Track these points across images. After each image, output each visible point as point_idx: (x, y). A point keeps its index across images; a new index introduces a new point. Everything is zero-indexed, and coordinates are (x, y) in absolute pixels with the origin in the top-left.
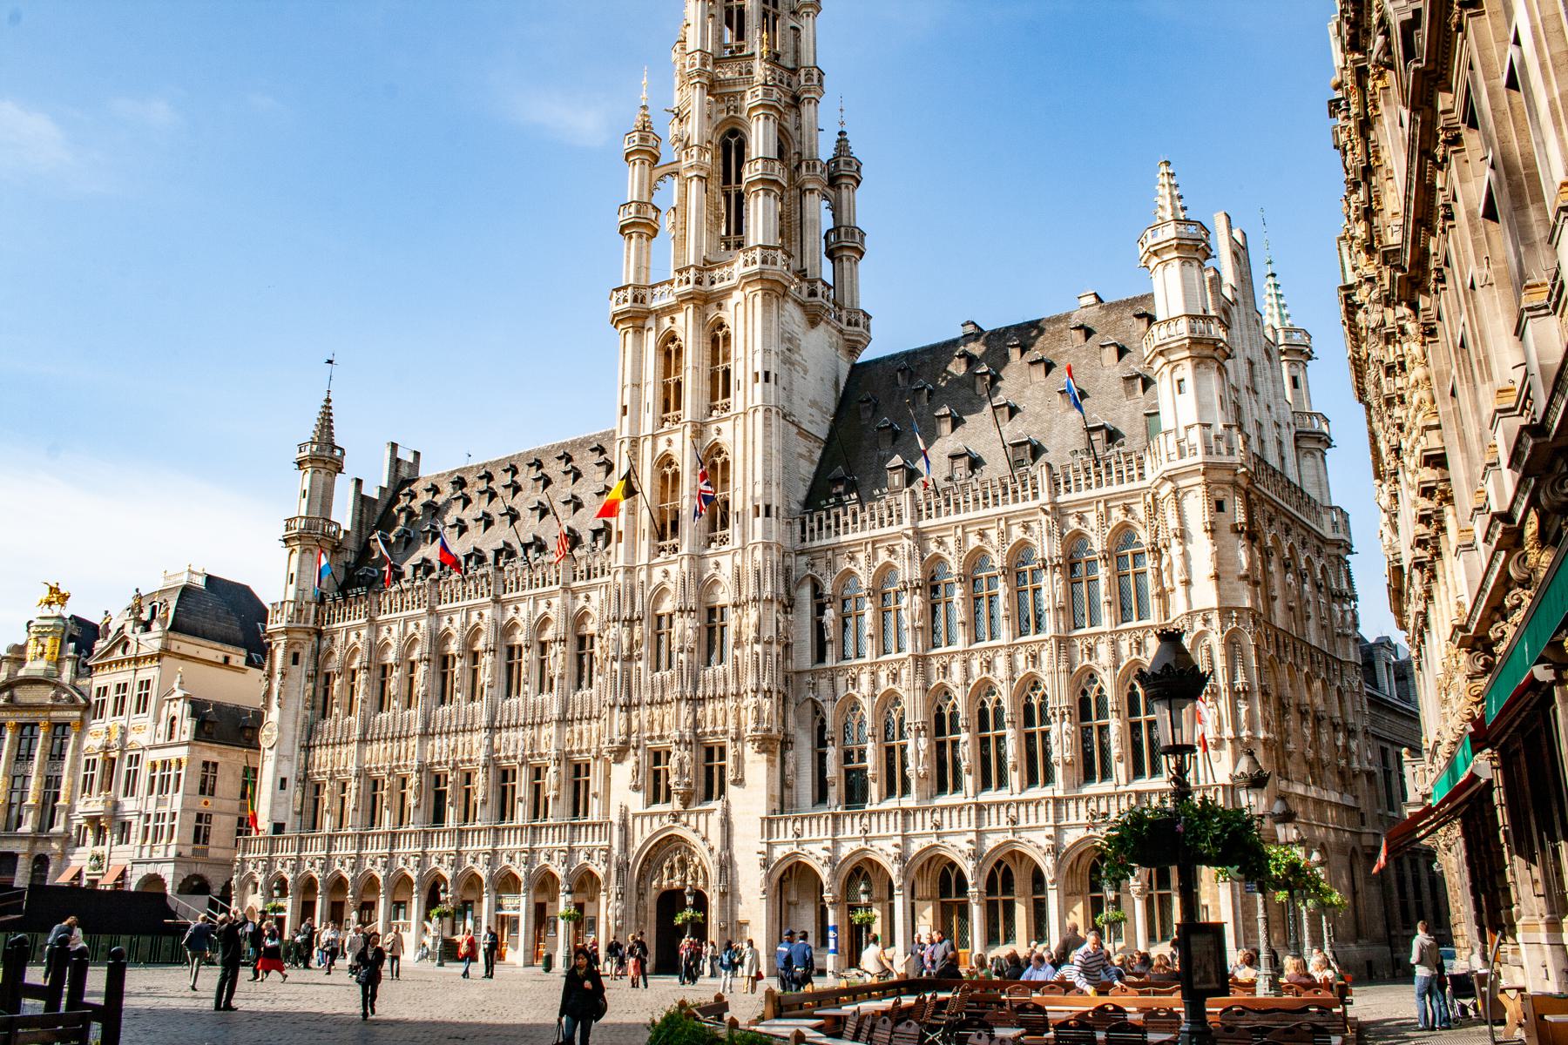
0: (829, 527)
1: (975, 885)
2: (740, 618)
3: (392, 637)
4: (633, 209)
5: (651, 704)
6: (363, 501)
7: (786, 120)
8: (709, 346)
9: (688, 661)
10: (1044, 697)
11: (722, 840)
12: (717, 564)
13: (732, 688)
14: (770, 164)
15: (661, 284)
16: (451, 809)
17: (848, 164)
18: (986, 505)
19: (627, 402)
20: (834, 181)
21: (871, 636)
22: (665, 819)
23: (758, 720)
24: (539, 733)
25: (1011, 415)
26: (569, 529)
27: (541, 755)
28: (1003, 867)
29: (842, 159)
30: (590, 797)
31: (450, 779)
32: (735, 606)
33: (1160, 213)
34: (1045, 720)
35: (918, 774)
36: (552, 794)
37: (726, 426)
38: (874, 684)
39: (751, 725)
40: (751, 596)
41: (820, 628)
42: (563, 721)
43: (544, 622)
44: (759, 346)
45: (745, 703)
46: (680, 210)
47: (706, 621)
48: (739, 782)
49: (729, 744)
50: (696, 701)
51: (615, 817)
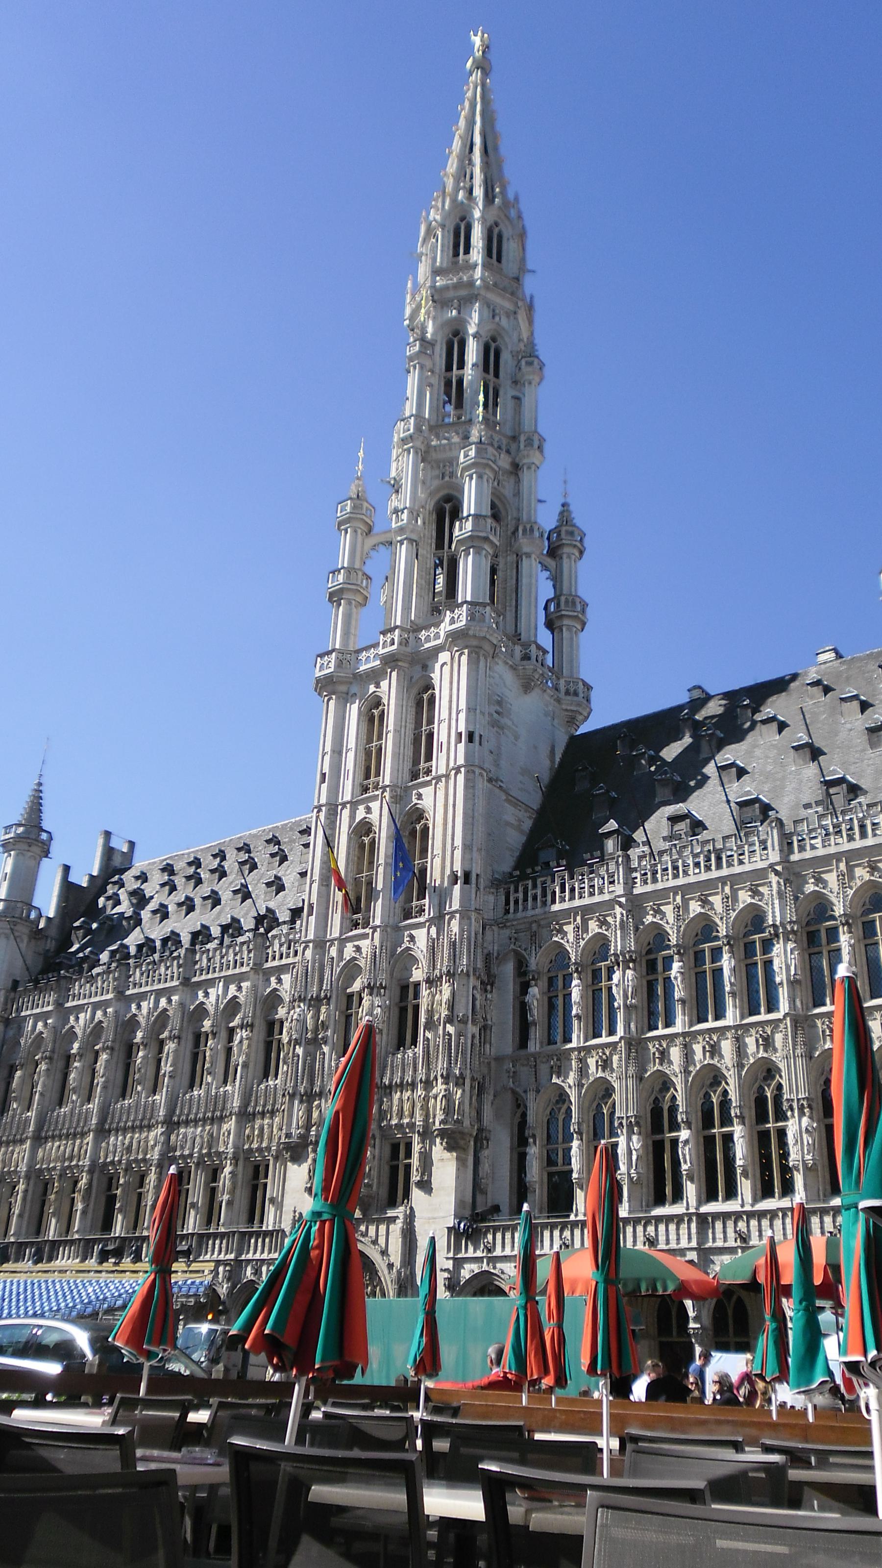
0: (535, 898)
1: (696, 1319)
2: (434, 996)
3: (80, 1023)
6: (69, 889)
7: (504, 487)
10: (780, 1087)
11: (403, 1255)
12: (412, 938)
13: (421, 1074)
14: (482, 521)
15: (367, 649)
16: (120, 1217)
17: (571, 534)
19: (326, 769)
20: (553, 552)
24: (220, 1128)
25: (739, 777)
27: (219, 1154)
28: (734, 1298)
31: (122, 1181)
32: (430, 982)
34: (781, 1116)
35: (630, 1179)
36: (226, 1197)
37: (425, 791)
39: (440, 1116)
40: (444, 969)
41: (523, 1009)
42: (246, 1116)
43: (233, 1006)
44: (463, 705)
45: (434, 1091)
47: (397, 999)
48: (426, 1186)
49: (416, 1138)
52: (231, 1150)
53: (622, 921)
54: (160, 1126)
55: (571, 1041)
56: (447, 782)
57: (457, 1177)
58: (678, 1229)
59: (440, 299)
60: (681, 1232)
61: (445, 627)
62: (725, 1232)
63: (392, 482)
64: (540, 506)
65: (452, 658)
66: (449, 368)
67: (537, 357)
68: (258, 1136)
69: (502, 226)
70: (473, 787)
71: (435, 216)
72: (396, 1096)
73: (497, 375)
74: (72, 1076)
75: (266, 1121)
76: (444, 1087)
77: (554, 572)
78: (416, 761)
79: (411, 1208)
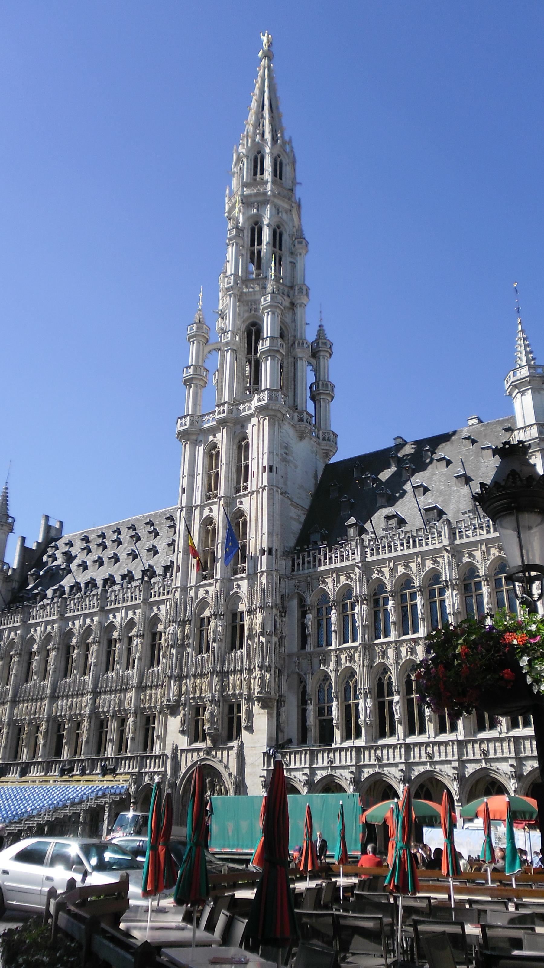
0: (309, 562)
2: (252, 620)
3: (38, 633)
4: (191, 371)
5: (195, 676)
6: (25, 551)
8: (236, 452)
9: (219, 648)
11: (238, 768)
12: (239, 586)
13: (246, 665)
14: (275, 341)
15: (209, 414)
16: (66, 748)
17: (325, 344)
18: (408, 547)
19: (185, 486)
20: (315, 354)
21: (335, 632)
22: (201, 754)
23: (262, 686)
24: (125, 696)
26: (149, 566)
27: (125, 710)
28: (425, 789)
29: (320, 341)
30: (155, 738)
31: (66, 727)
32: (250, 612)
33: (519, 362)
35: (366, 723)
36: (130, 736)
37: (245, 500)
38: (338, 662)
39: (257, 689)
40: (258, 605)
41: (303, 627)
43: (131, 624)
44: (266, 450)
45: (254, 675)
46: (220, 371)
47: (231, 622)
48: (250, 729)
49: (243, 702)
50: (224, 675)
51: (169, 752)
52: (133, 708)
53: (360, 577)
54: (89, 694)
55: (331, 645)
56: (257, 495)
57: (268, 724)
58: (394, 752)
59: (247, 202)
60: (396, 753)
61: (255, 403)
62: (420, 754)
63: (220, 312)
64: (307, 326)
65: (259, 422)
66: (252, 244)
67: (304, 239)
68: (149, 700)
69: (282, 157)
70: (273, 498)
71: (242, 150)
72: (232, 678)
73: (280, 249)
74: (34, 664)
75: (153, 691)
76: (259, 672)
77: (315, 367)
78: (238, 482)
79: (242, 742)
